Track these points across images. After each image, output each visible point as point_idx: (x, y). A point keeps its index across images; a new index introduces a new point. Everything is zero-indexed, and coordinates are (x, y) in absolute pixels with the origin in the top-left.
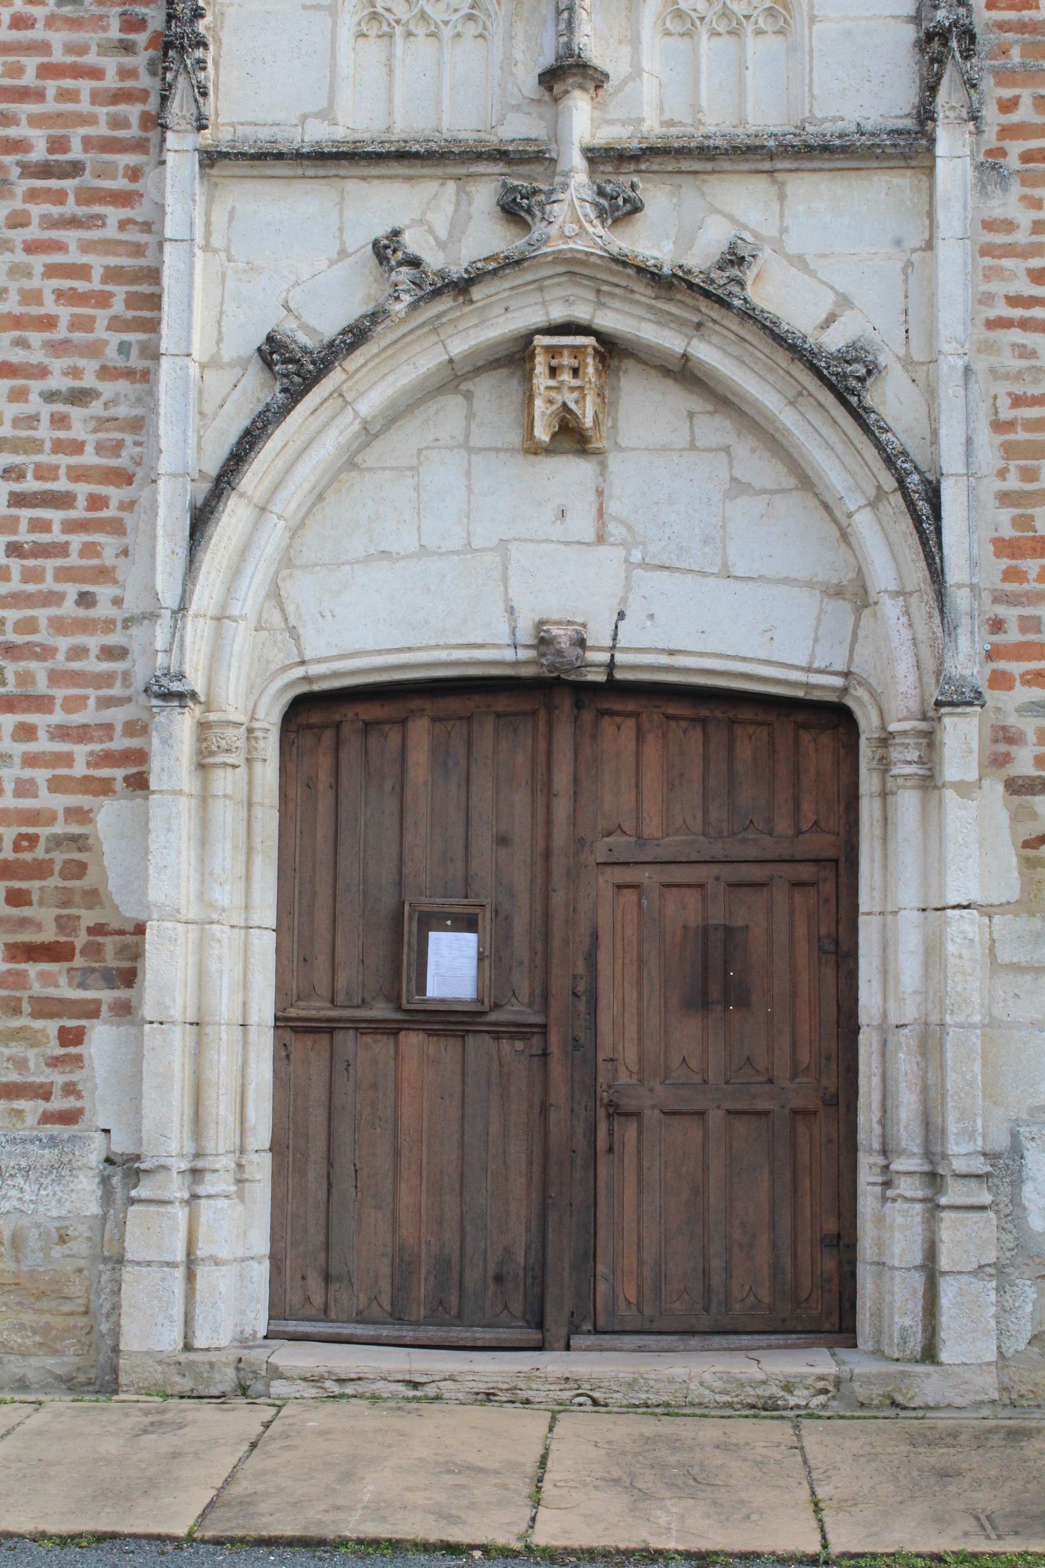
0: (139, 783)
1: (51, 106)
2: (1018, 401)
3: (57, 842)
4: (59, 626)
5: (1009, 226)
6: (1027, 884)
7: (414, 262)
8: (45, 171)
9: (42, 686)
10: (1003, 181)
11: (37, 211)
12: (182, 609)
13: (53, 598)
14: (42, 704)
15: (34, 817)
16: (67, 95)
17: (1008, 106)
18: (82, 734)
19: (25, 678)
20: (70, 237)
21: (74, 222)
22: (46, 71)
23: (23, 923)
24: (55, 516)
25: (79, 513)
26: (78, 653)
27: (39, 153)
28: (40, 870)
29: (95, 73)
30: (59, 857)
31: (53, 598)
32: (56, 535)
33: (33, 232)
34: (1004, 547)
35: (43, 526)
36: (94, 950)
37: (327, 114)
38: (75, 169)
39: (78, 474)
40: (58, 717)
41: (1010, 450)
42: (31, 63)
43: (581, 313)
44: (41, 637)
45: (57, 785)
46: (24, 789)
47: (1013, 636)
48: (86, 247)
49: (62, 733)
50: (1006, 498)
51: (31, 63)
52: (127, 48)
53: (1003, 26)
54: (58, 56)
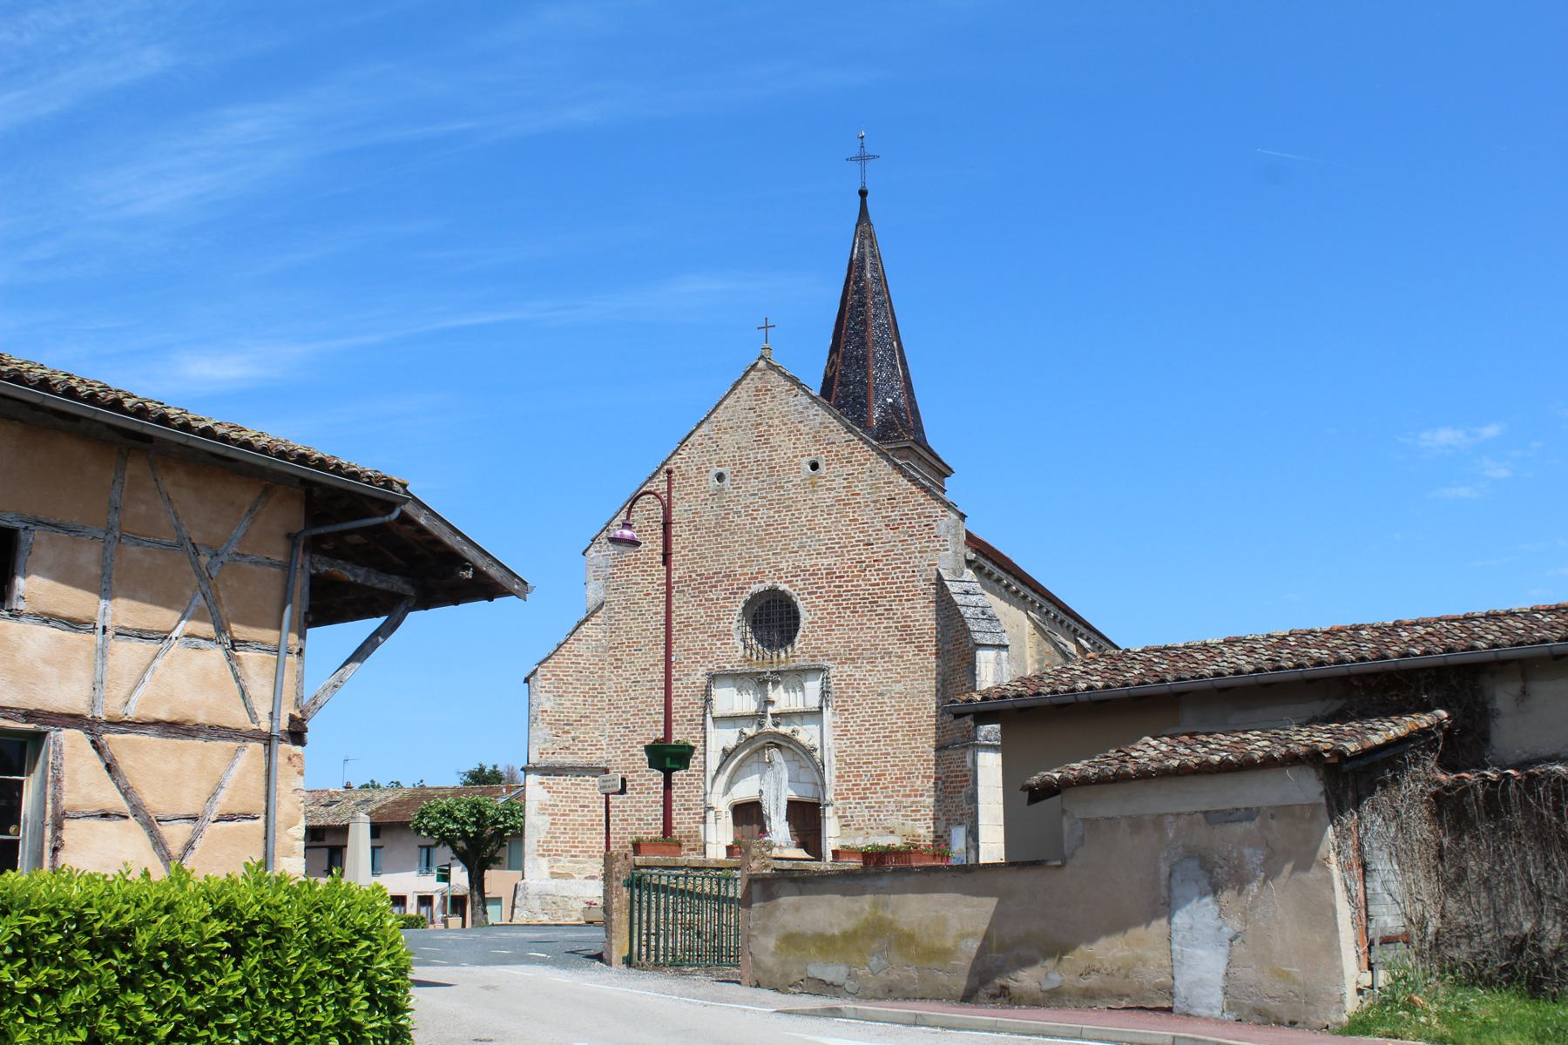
0: (705, 822)
1: (690, 709)
2: (839, 752)
3: (694, 832)
4: (694, 796)
5: (837, 722)
6: (841, 833)
7: (745, 734)
8: (690, 720)
9: (691, 806)
10: (836, 715)
11: (689, 727)
12: (711, 793)
13: (693, 792)
14: (691, 809)
15: (690, 828)
16: (693, 708)
17: (837, 702)
18: (697, 814)
19: (689, 805)
20: (694, 731)
21: (694, 729)
22: (690, 704)
23: (690, 845)
24: (692, 778)
25: (696, 777)
26: (696, 800)
27: (689, 717)
28: (692, 836)
29: (697, 704)
30: (694, 834)
31: (693, 792)
32: (693, 781)
33: (688, 730)
34: (837, 777)
35: (690, 780)
36: (700, 849)
37: (732, 709)
38: (694, 720)
39: (696, 771)
40: (693, 811)
41: (838, 761)
42: (687, 702)
43: (772, 740)
44: (691, 798)
45: (694, 822)
46: (689, 823)
47: (838, 792)
48: (697, 733)
49: (694, 814)
50: (837, 769)
51: (687, 702)
52: (701, 699)
53: (836, 688)
54: (692, 701)
